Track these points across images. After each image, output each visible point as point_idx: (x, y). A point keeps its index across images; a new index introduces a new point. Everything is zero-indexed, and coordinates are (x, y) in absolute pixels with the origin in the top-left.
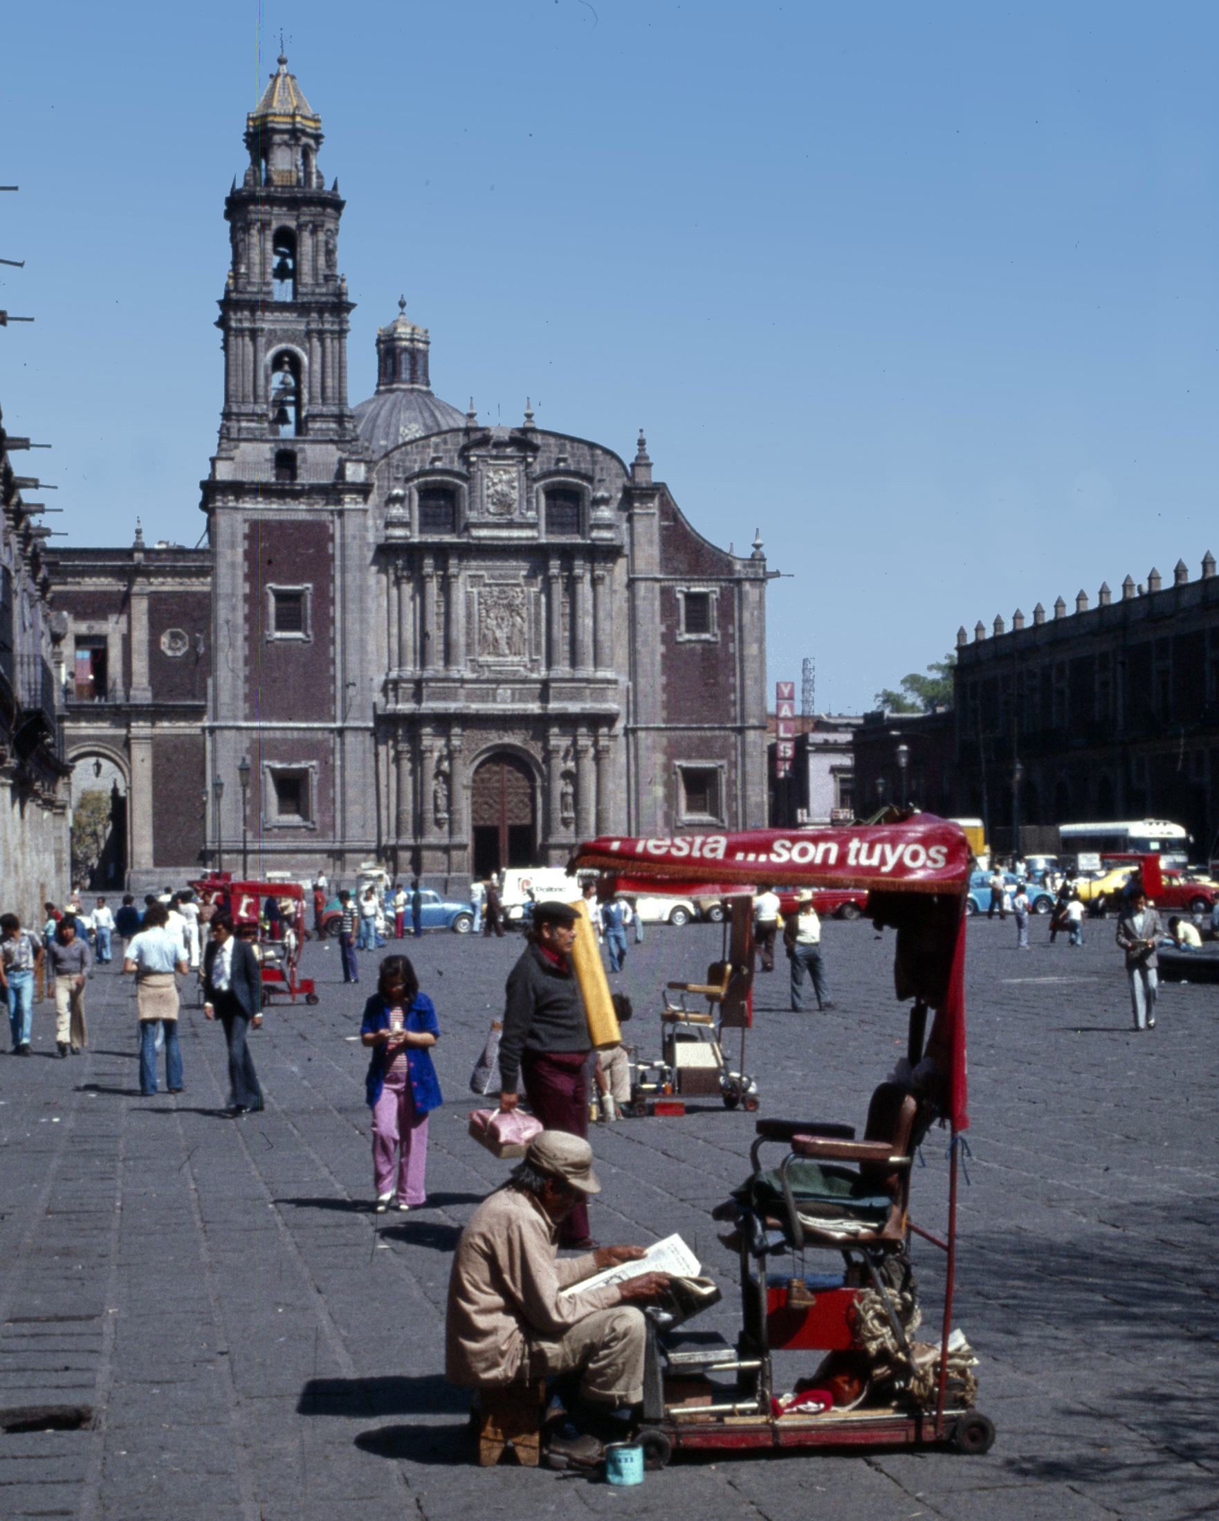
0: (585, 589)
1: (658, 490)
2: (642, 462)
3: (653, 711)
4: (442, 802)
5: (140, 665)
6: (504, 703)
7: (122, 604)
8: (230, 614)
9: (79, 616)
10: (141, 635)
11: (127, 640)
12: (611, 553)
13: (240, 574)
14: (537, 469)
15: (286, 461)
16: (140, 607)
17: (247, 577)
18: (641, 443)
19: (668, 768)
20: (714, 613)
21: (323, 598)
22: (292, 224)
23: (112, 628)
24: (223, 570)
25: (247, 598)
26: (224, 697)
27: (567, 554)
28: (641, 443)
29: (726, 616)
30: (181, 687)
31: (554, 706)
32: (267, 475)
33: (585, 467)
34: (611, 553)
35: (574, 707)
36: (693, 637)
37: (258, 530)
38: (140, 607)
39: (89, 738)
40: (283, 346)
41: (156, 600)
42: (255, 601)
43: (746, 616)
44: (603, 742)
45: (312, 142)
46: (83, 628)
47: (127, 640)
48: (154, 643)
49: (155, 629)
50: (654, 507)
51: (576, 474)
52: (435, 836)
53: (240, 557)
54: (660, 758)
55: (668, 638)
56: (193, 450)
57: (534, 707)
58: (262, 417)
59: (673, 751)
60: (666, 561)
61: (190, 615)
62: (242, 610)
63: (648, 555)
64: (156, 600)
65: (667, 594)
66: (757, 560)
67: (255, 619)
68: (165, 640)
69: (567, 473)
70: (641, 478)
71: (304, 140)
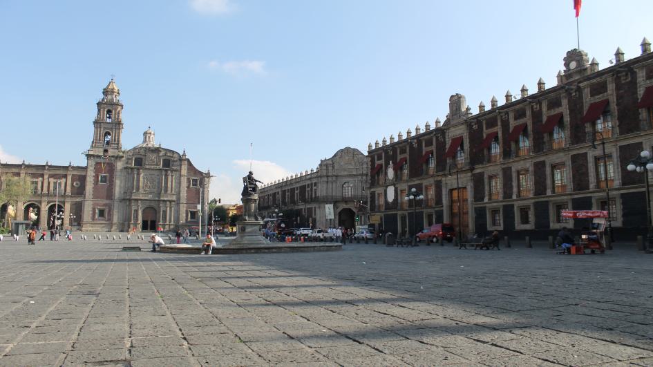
0: (170, 178)
1: (188, 160)
2: (184, 155)
5: (69, 188)
9: (55, 178)
15: (106, 151)
16: (69, 178)
23: (63, 181)
26: (87, 194)
35: (166, 199)
38: (69, 178)
42: (97, 177)
48: (72, 184)
49: (73, 181)
50: (186, 162)
54: (185, 209)
55: (188, 187)
56: (87, 146)
57: (157, 199)
60: (188, 172)
61: (83, 179)
63: (184, 171)
65: (188, 180)
66: (209, 173)
67: (96, 182)
70: (184, 158)
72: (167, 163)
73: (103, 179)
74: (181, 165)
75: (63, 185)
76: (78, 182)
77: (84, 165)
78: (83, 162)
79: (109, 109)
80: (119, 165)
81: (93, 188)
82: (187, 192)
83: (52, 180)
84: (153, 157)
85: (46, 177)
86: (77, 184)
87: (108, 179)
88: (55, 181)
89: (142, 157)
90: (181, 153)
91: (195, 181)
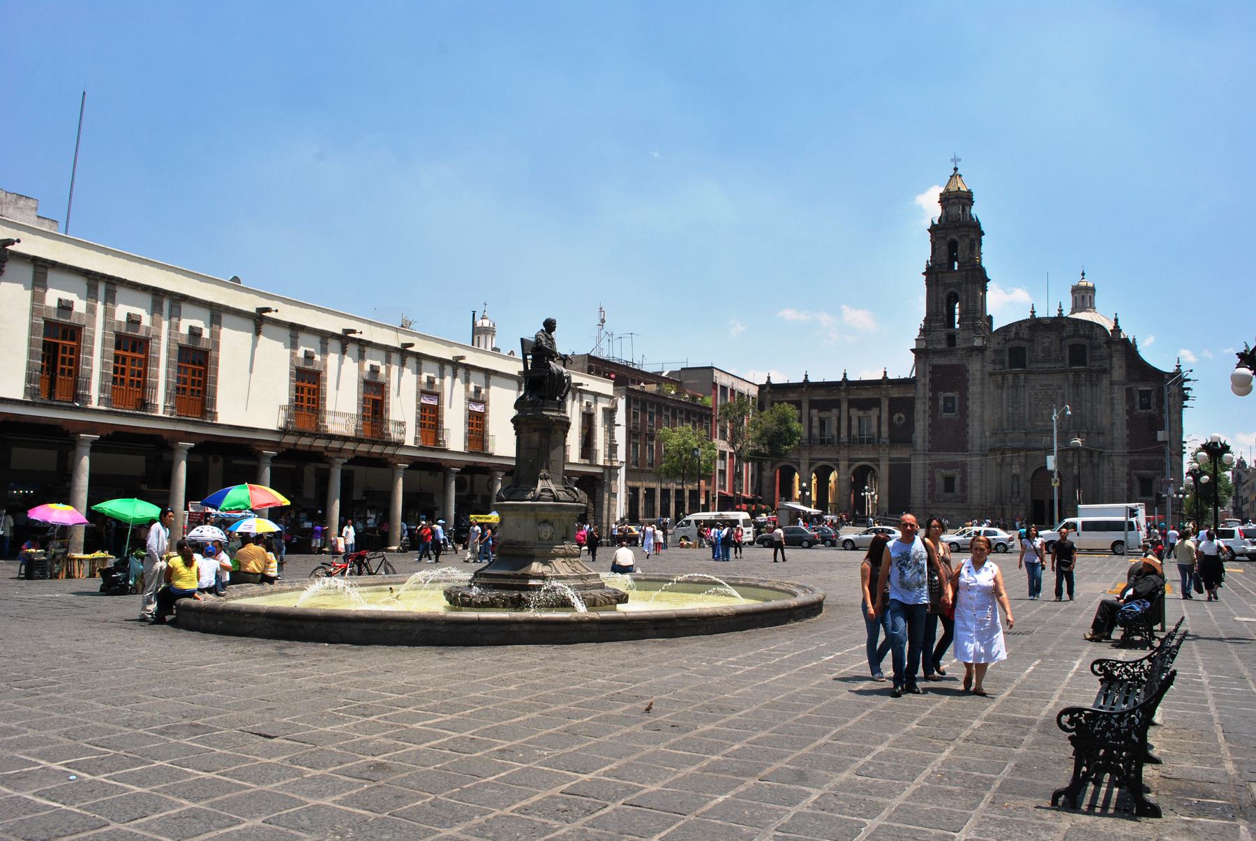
2: (1117, 329)
5: (885, 429)
7: (876, 403)
9: (859, 409)
10: (885, 416)
11: (879, 418)
18: (1116, 320)
19: (1128, 474)
20: (1153, 400)
21: (964, 398)
22: (955, 237)
23: (874, 413)
24: (919, 386)
27: (1077, 373)
28: (1116, 320)
29: (1161, 401)
30: (901, 436)
32: (943, 346)
34: (1104, 371)
36: (1144, 411)
37: (936, 369)
39: (861, 460)
40: (952, 289)
41: (892, 401)
42: (934, 399)
44: (1095, 461)
47: (879, 418)
51: (1084, 336)
55: (1129, 412)
59: (1133, 466)
60: (1128, 374)
62: (928, 403)
63: (1118, 373)
64: (892, 401)
65: (1129, 391)
66: (1178, 371)
72: (1078, 355)
73: (949, 405)
75: (874, 422)
76: (902, 416)
79: (956, 248)
80: (975, 368)
82: (1130, 424)
83: (855, 413)
84: (1046, 340)
85: (844, 406)
86: (900, 419)
88: (861, 413)
90: (1109, 326)
91: (1144, 394)
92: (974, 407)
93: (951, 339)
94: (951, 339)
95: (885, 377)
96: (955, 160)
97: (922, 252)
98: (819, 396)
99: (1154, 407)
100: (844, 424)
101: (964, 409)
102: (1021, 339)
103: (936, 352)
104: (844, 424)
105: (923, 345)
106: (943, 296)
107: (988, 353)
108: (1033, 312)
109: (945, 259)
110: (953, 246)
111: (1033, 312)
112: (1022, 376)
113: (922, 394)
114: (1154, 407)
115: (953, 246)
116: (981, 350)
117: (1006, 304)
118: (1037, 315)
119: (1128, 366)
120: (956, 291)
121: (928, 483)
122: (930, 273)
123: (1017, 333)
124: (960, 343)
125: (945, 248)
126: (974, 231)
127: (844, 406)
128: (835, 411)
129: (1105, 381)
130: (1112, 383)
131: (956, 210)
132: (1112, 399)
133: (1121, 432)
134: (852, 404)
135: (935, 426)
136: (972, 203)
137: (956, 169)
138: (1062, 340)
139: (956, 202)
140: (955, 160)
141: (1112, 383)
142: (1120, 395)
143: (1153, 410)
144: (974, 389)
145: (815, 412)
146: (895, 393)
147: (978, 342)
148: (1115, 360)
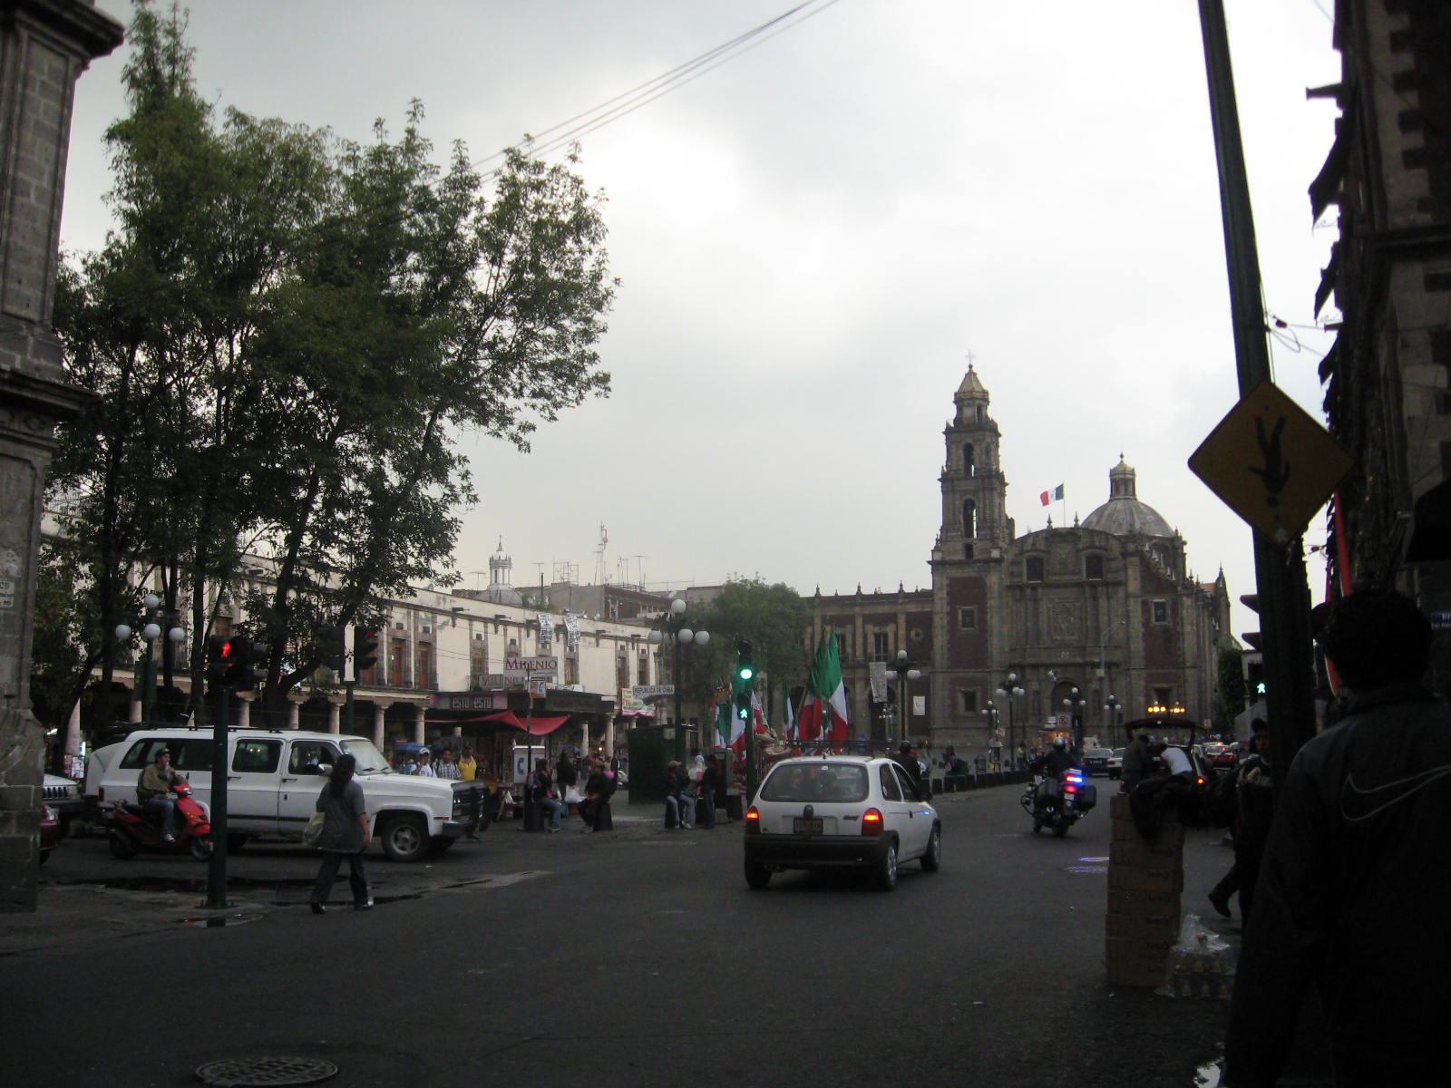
0: (1103, 603)
3: (1138, 660)
4: (1036, 704)
6: (1065, 656)
7: (892, 618)
8: (940, 622)
10: (902, 632)
11: (896, 634)
12: (1118, 584)
13: (945, 602)
14: (1080, 546)
17: (948, 604)
20: (1169, 612)
21: (983, 611)
22: (970, 441)
23: (890, 629)
25: (948, 613)
26: (938, 658)
27: (1094, 586)
29: (1175, 613)
31: (1088, 659)
32: (961, 557)
33: (1103, 544)
34: (1118, 584)
36: (1158, 623)
37: (953, 582)
40: (968, 497)
42: (952, 614)
43: (1184, 612)
45: (981, 402)
46: (877, 629)
47: (896, 634)
49: (908, 629)
50: (1135, 560)
51: (1100, 548)
52: (1031, 722)
53: (945, 595)
54: (1142, 683)
55: (1146, 624)
57: (1079, 660)
58: (958, 530)
59: (1149, 679)
60: (1143, 587)
62: (946, 618)
63: (1134, 585)
65: (1145, 604)
68: (913, 633)
69: (1096, 548)
71: (977, 402)
74: (1126, 569)
76: (921, 632)
77: (930, 587)
78: (921, 579)
80: (994, 580)
81: (949, 642)
83: (871, 629)
84: (1063, 551)
85: (859, 622)
86: (917, 635)
87: (976, 616)
88: (877, 629)
89: (1043, 555)
91: (1159, 606)
92: (994, 621)
93: (969, 549)
94: (969, 549)
95: (901, 591)
96: (970, 356)
97: (936, 456)
98: (832, 611)
99: (1169, 619)
100: (859, 640)
101: (983, 622)
102: (1037, 550)
103: (953, 564)
104: (859, 640)
105: (938, 556)
106: (959, 503)
107: (1004, 564)
108: (1049, 522)
109: (962, 464)
110: (969, 449)
111: (1049, 522)
112: (1040, 590)
113: (941, 606)
114: (1169, 619)
115: (969, 449)
116: (999, 561)
117: (1026, 513)
118: (1054, 525)
119: (1143, 578)
120: (973, 498)
121: (948, 702)
122: (946, 479)
123: (1034, 545)
124: (977, 554)
125: (961, 453)
126: (991, 430)
127: (859, 622)
128: (849, 627)
129: (1121, 594)
130: (1127, 596)
131: (969, 412)
132: (1128, 612)
133: (1138, 646)
134: (868, 619)
135: (954, 642)
136: (988, 402)
137: (971, 367)
138: (1078, 551)
139: (971, 400)
140: (970, 356)
141: (1127, 596)
142: (1135, 608)
143: (1168, 623)
144: (993, 603)
145: (828, 628)
146: (912, 608)
147: (995, 554)
148: (1130, 572)
